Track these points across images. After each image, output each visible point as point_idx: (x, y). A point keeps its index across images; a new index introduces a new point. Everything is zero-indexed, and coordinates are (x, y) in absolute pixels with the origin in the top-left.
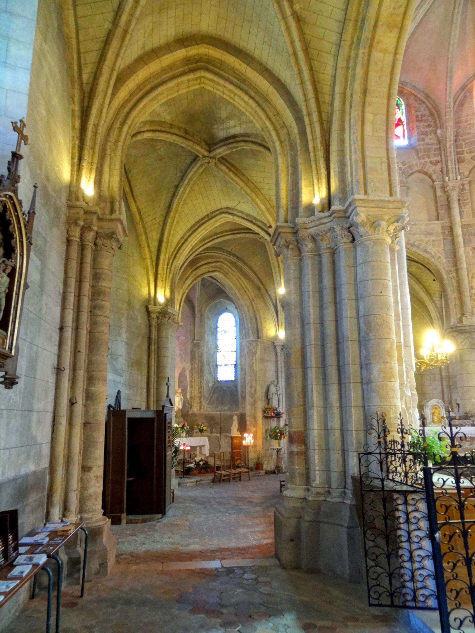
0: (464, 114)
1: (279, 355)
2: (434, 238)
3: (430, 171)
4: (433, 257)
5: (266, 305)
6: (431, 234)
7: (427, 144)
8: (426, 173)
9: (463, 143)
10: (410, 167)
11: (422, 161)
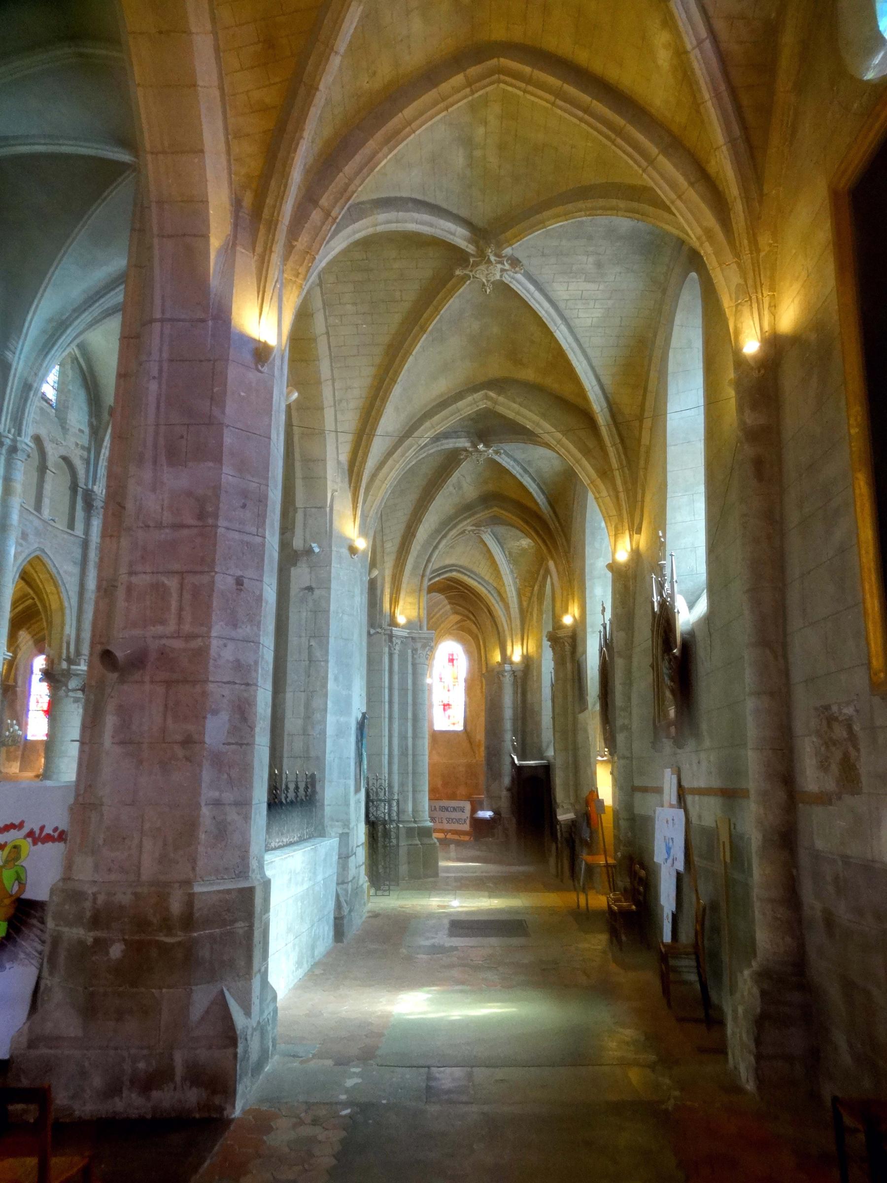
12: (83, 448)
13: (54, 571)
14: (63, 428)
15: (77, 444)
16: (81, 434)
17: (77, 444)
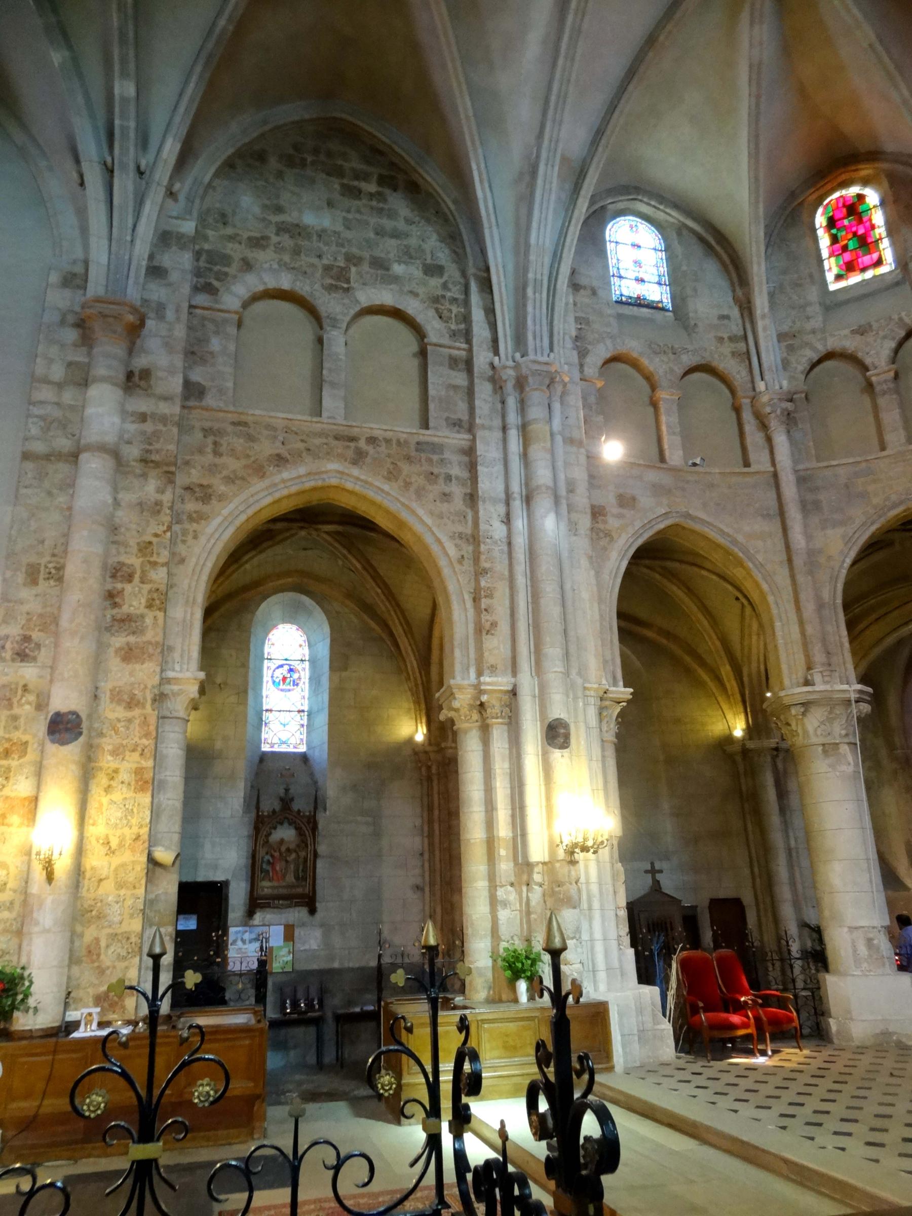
13: (721, 540)
14: (686, 328)
15: (721, 340)
16: (726, 322)
17: (721, 340)
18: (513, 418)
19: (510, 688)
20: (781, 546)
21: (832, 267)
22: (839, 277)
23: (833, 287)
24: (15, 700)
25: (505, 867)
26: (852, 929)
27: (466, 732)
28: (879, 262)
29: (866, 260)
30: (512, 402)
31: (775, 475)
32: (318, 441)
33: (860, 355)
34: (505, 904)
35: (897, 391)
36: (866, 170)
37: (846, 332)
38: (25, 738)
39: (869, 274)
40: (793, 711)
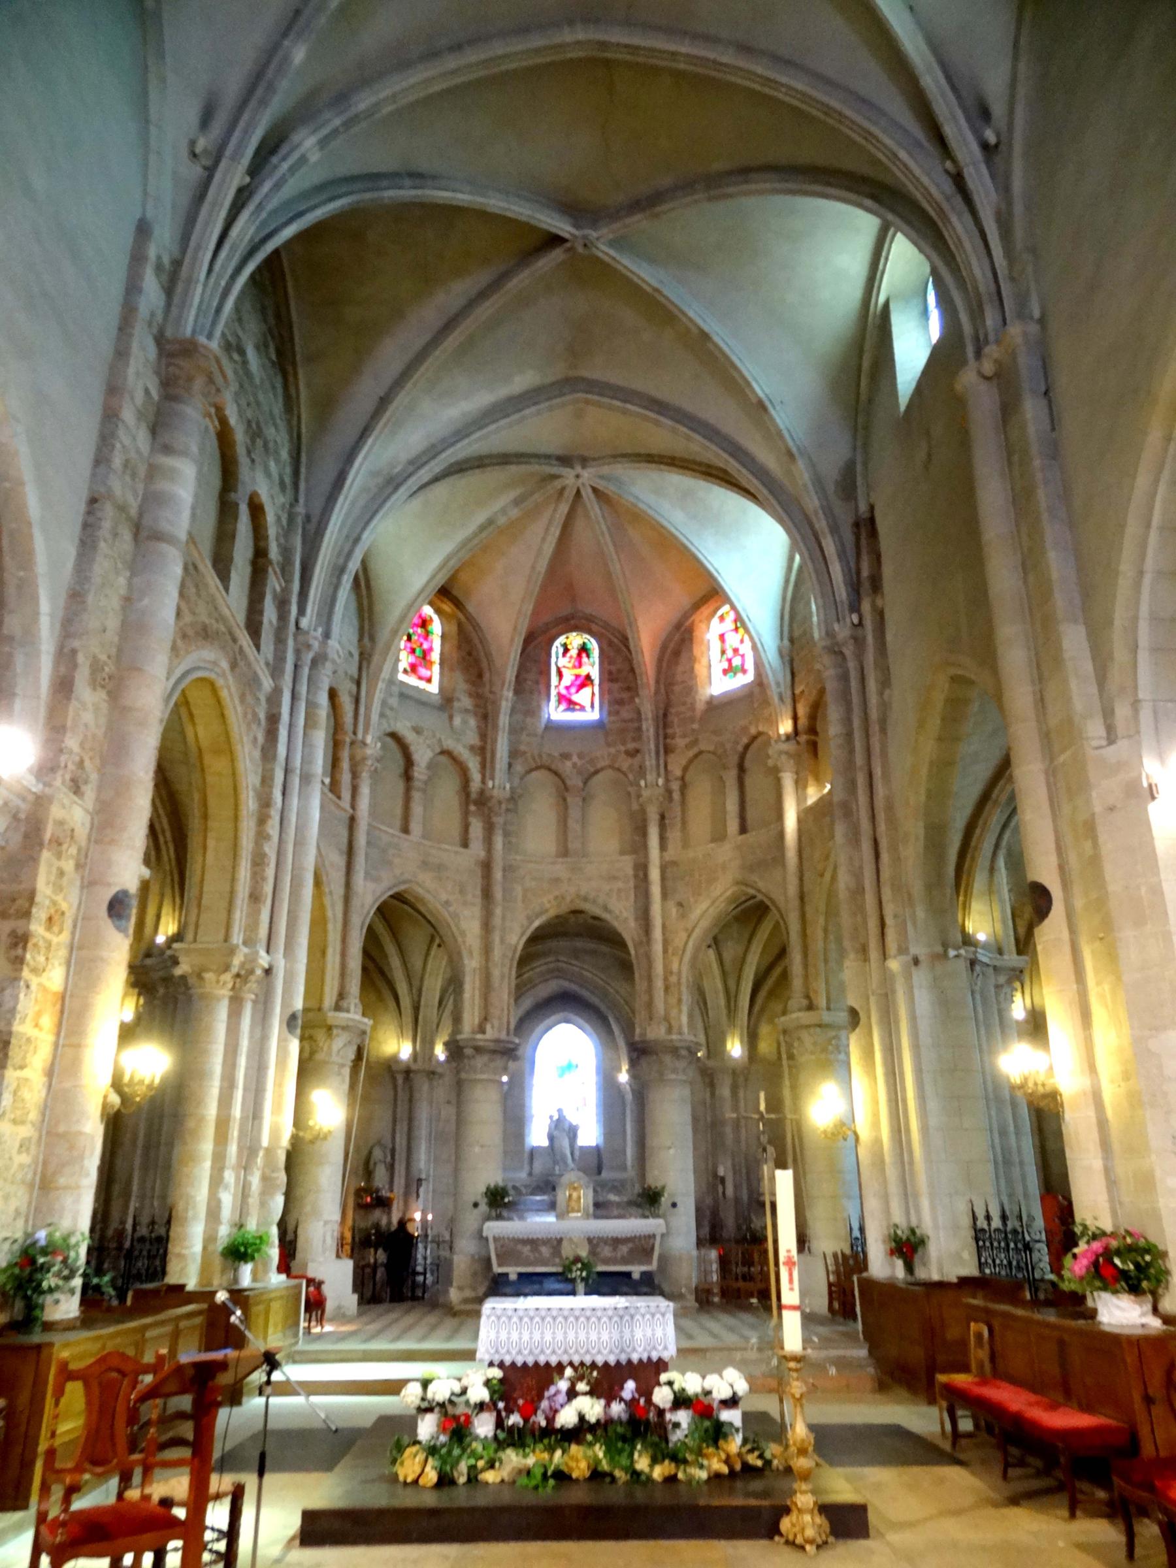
0: (680, 669)
1: (399, 1089)
2: (620, 885)
3: (624, 768)
4: (617, 917)
5: (381, 998)
6: (615, 878)
7: (625, 721)
8: (619, 770)
9: (676, 720)
10: (592, 761)
11: (612, 750)
12: (352, 678)
18: (303, 689)
19: (266, 966)
20: (343, 881)
21: (405, 660)
22: (405, 671)
23: (402, 677)
24: (65, 846)
25: (233, 1149)
26: (326, 1223)
27: (219, 1000)
28: (429, 680)
29: (423, 672)
30: (306, 671)
31: (352, 819)
32: (223, 629)
33: (412, 748)
34: (226, 1187)
35: (424, 791)
36: (447, 607)
37: (408, 724)
38: (64, 906)
39: (422, 685)
40: (335, 1032)
